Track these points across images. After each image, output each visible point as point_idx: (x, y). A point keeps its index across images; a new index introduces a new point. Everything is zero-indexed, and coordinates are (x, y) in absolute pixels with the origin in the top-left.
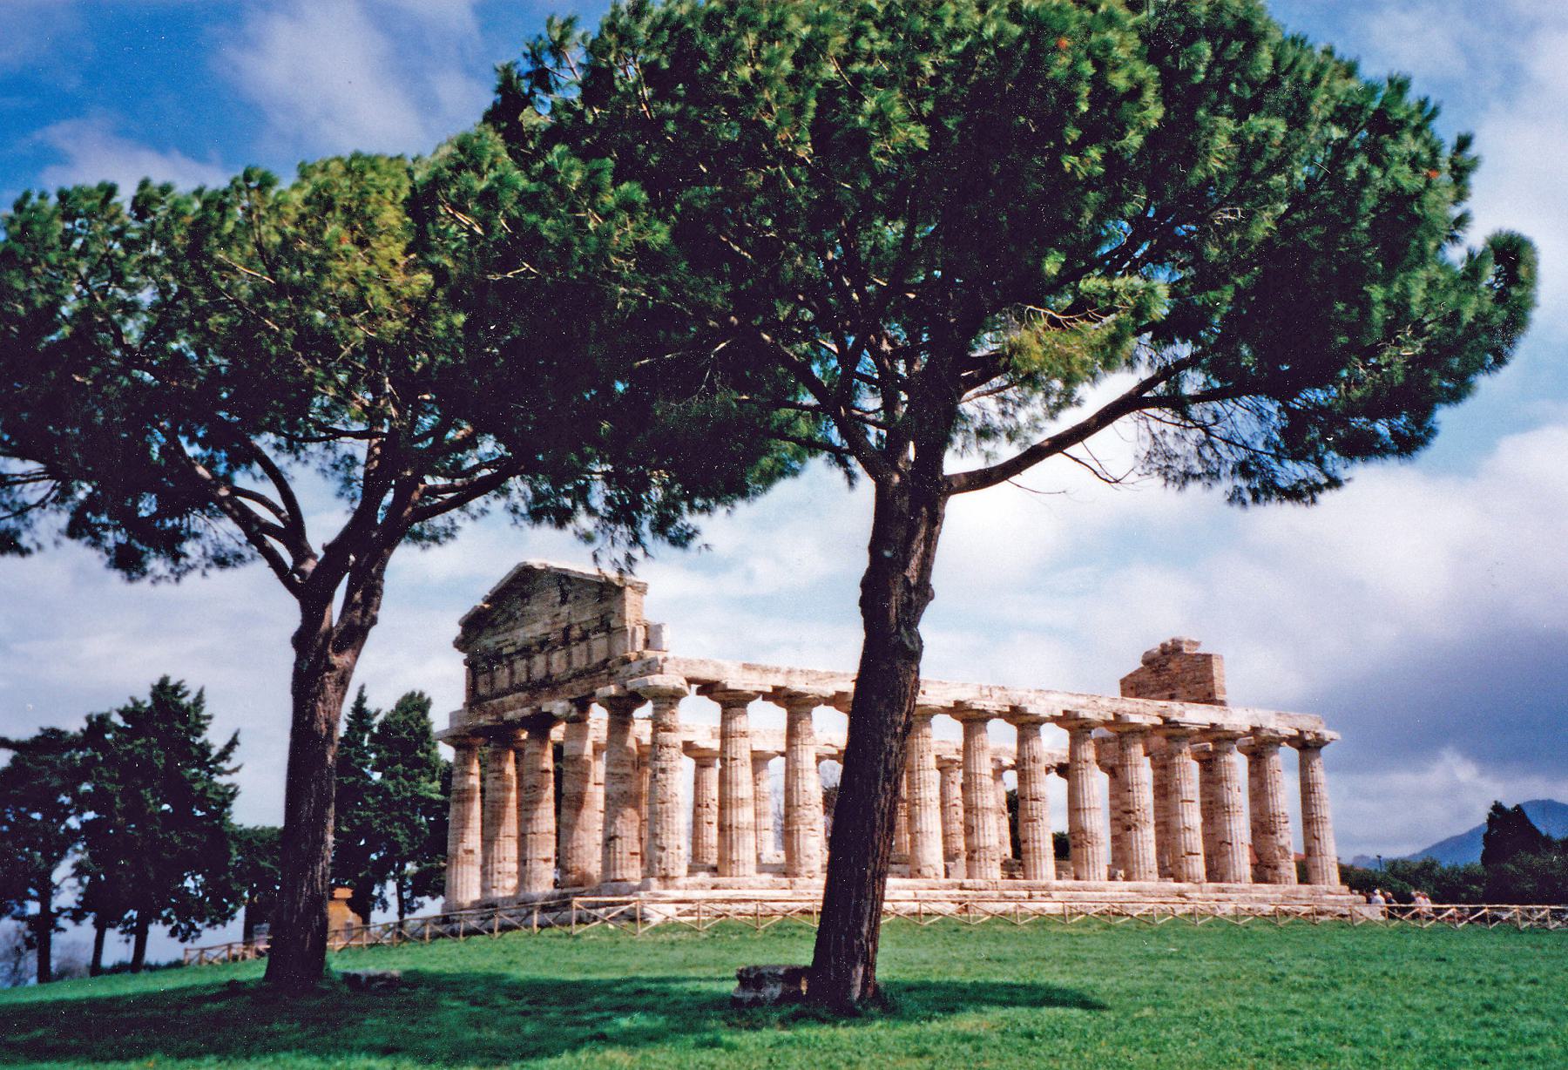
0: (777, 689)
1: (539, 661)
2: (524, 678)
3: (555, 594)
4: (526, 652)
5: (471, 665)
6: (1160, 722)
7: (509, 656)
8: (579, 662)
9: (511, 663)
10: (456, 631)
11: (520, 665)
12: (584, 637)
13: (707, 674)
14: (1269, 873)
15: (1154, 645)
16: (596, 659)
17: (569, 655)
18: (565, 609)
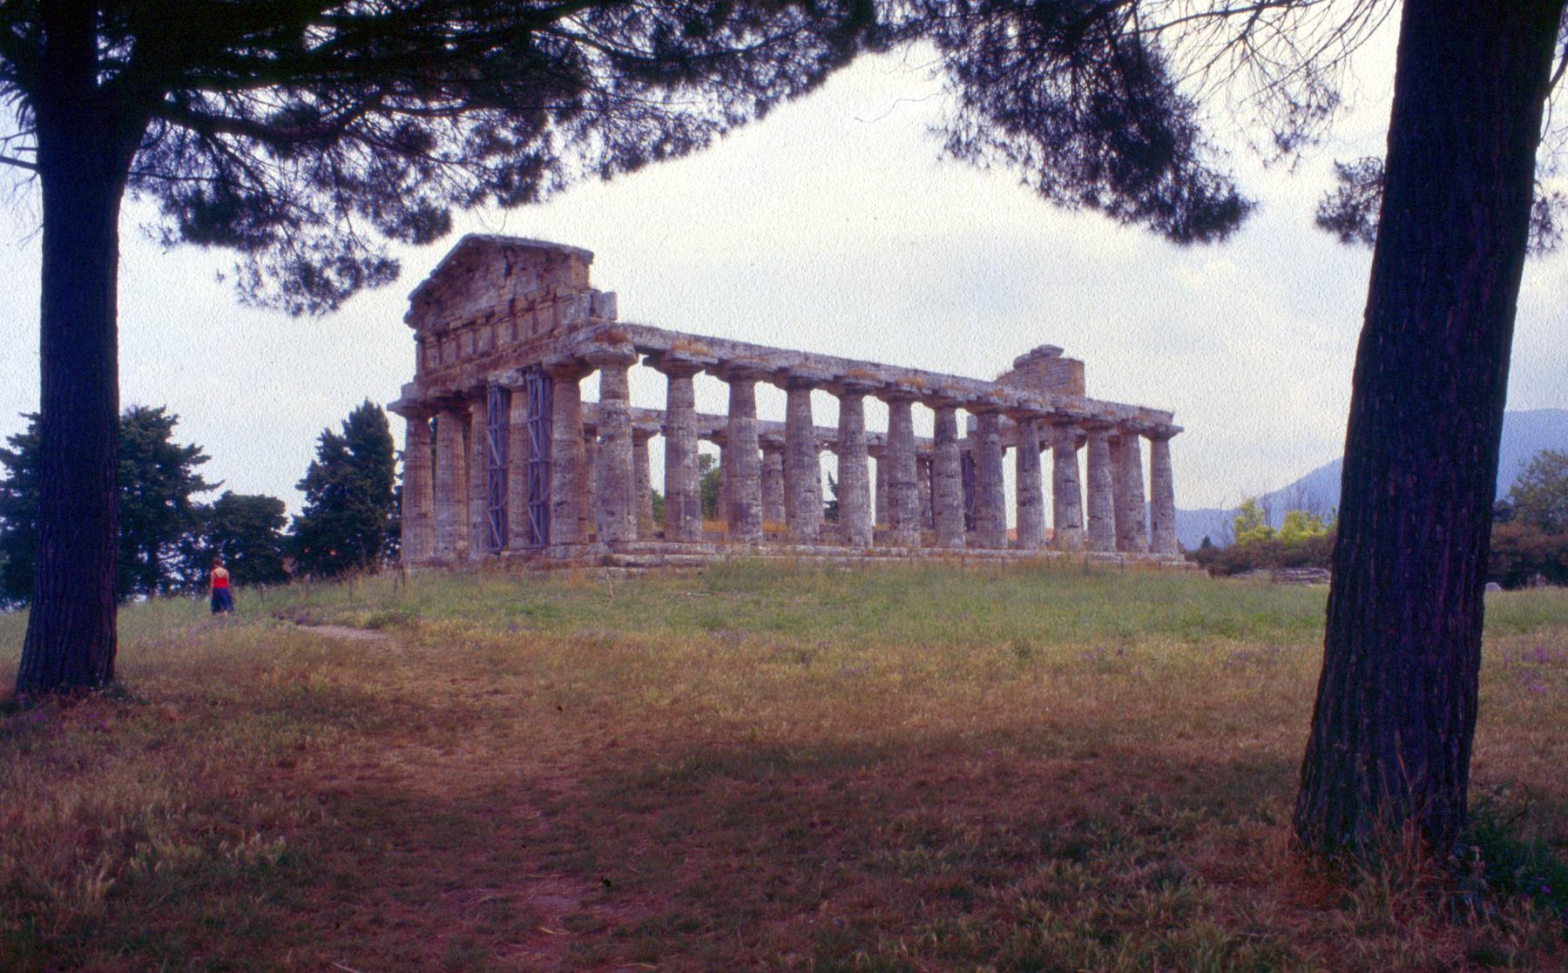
0: (722, 362)
1: (485, 333)
2: (470, 350)
3: (500, 266)
4: (471, 324)
5: (421, 340)
6: (1052, 410)
7: (457, 329)
8: (526, 334)
9: (458, 337)
10: (406, 306)
11: (466, 337)
12: (531, 308)
13: (656, 343)
14: (1126, 542)
15: (1025, 349)
16: (542, 330)
17: (515, 326)
18: (511, 282)
